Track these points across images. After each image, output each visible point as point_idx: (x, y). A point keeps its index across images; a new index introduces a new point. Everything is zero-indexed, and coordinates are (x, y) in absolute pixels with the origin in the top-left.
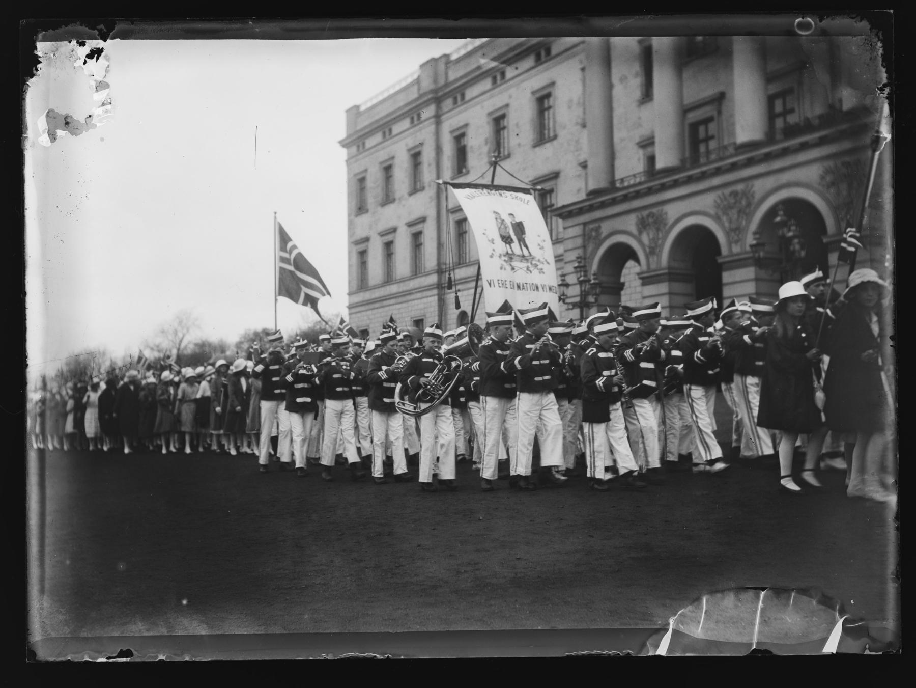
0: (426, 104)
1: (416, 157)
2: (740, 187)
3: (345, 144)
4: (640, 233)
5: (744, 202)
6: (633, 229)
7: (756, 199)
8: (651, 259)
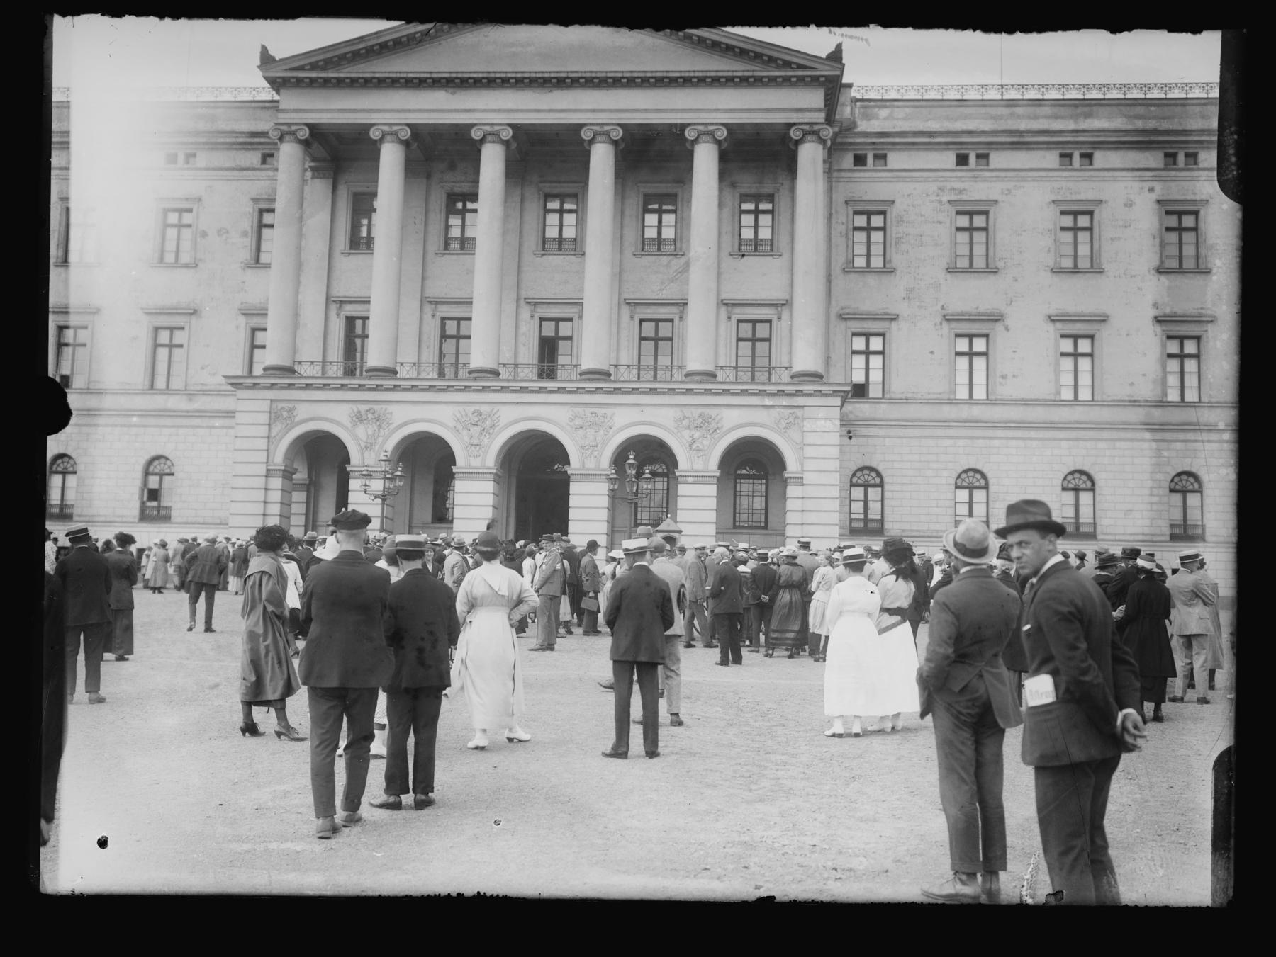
2: (484, 409)
4: (355, 425)
5: (488, 423)
6: (346, 421)
7: (502, 424)
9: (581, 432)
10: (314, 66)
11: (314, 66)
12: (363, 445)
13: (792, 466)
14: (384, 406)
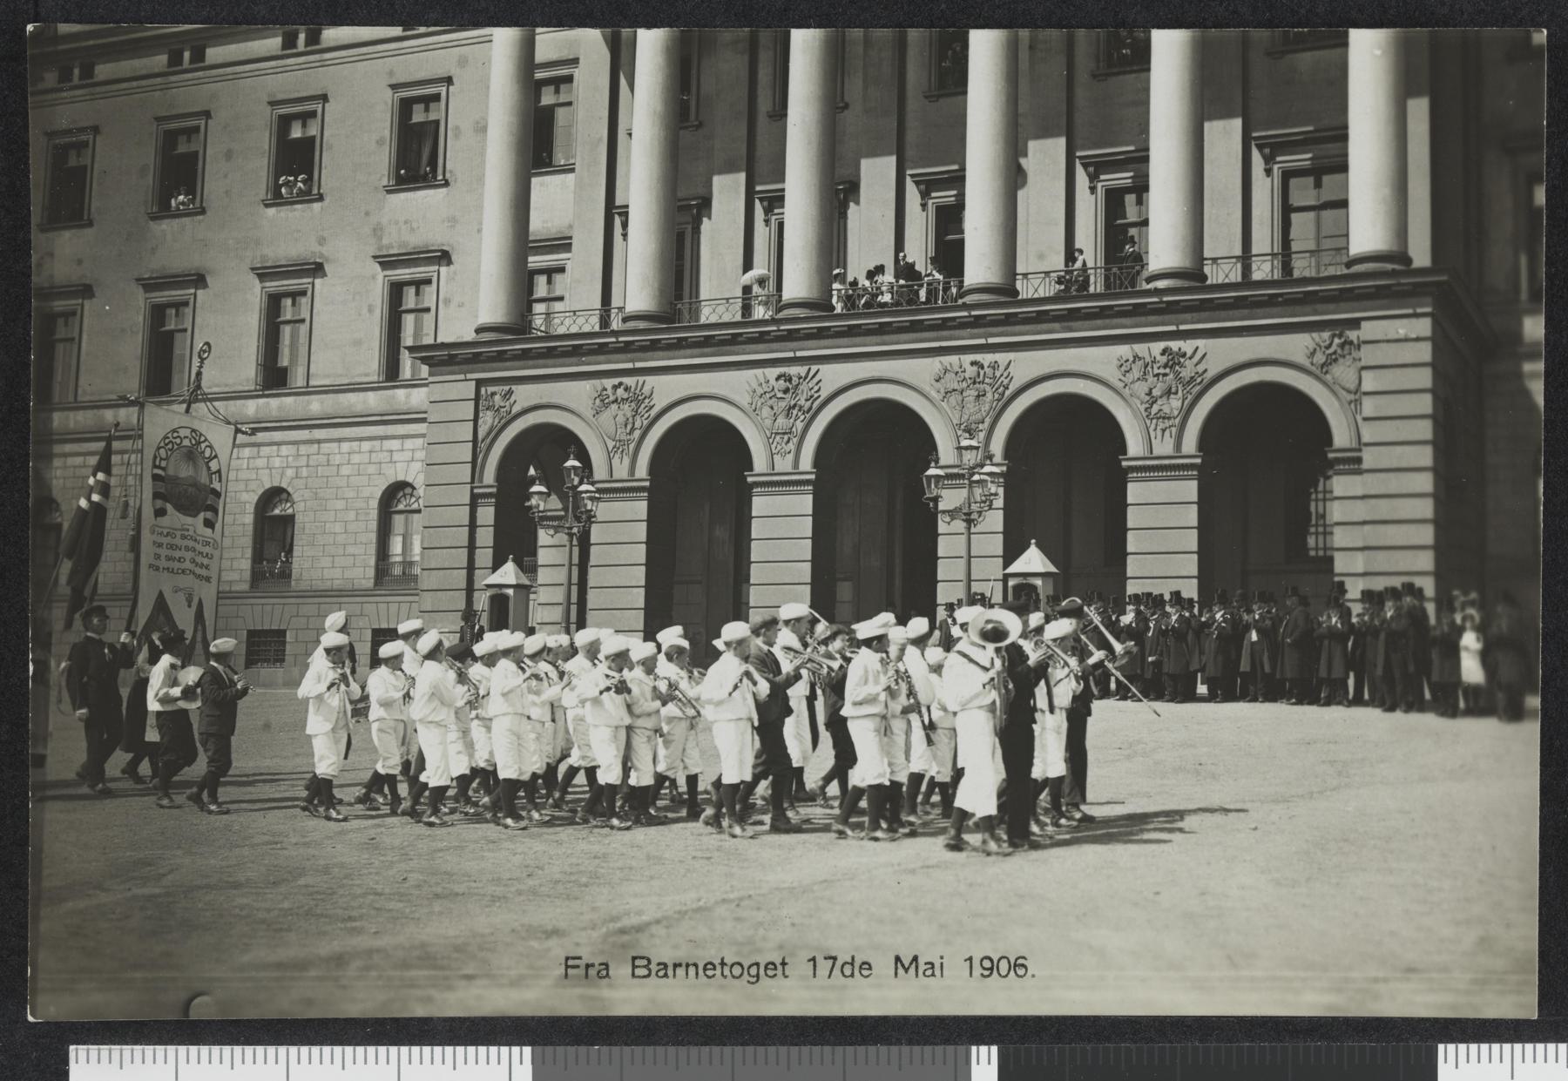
2: (794, 370)
8: (616, 461)
9: (954, 399)
12: (611, 444)
13: (1341, 437)
14: (641, 379)
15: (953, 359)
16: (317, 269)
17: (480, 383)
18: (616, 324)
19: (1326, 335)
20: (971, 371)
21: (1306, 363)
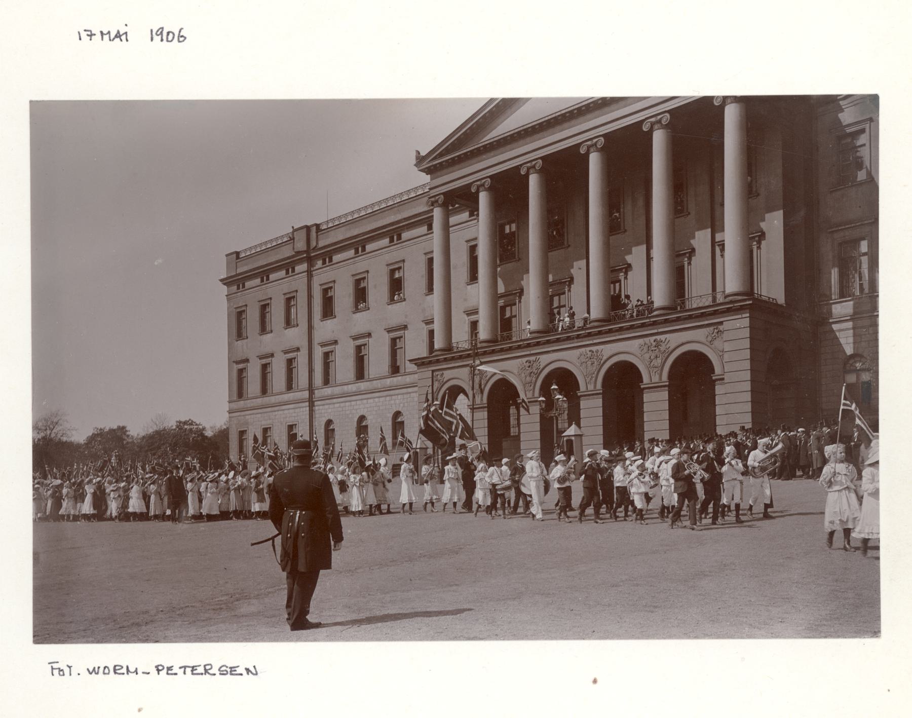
0: (300, 261)
1: (289, 301)
2: (532, 358)
3: (227, 282)
9: (584, 365)
10: (441, 155)
11: (441, 155)
13: (718, 370)
15: (583, 350)
16: (405, 327)
17: (433, 371)
18: (479, 345)
19: (712, 328)
20: (590, 354)
21: (703, 340)
